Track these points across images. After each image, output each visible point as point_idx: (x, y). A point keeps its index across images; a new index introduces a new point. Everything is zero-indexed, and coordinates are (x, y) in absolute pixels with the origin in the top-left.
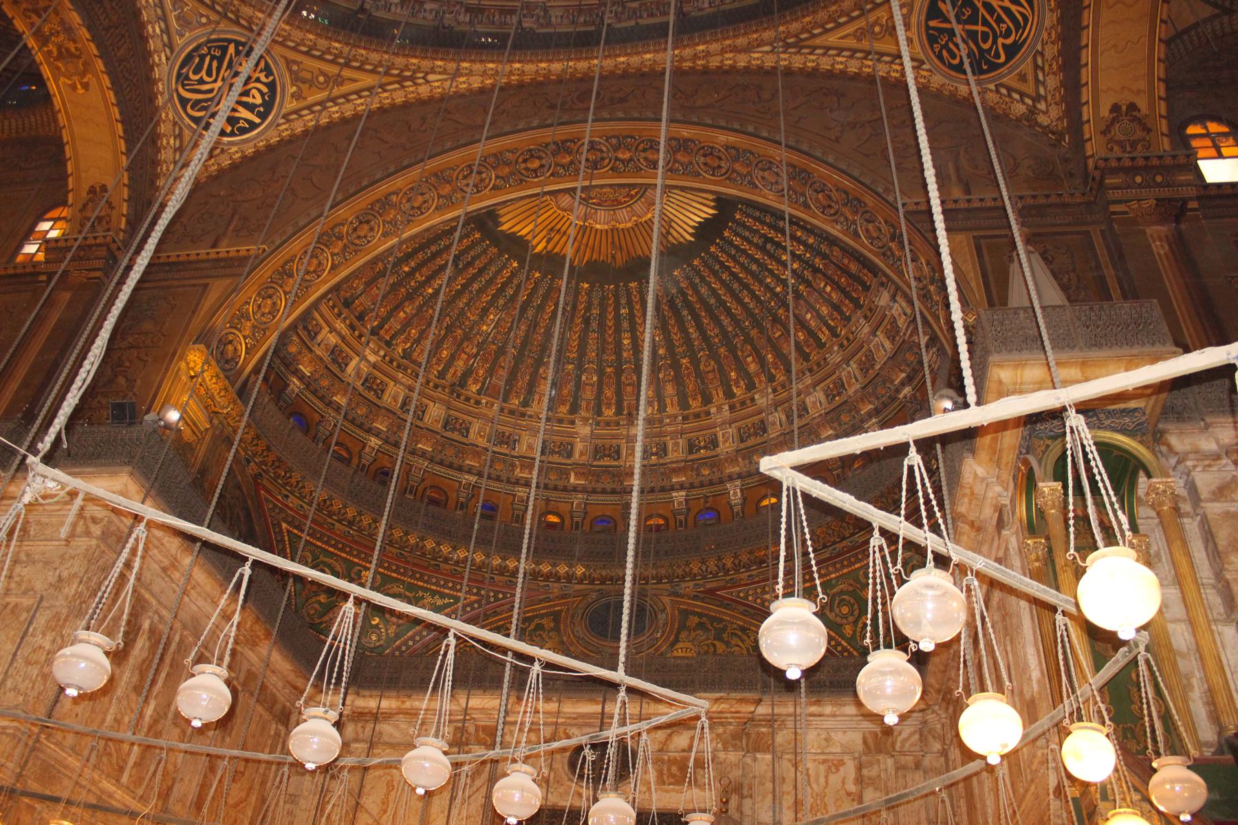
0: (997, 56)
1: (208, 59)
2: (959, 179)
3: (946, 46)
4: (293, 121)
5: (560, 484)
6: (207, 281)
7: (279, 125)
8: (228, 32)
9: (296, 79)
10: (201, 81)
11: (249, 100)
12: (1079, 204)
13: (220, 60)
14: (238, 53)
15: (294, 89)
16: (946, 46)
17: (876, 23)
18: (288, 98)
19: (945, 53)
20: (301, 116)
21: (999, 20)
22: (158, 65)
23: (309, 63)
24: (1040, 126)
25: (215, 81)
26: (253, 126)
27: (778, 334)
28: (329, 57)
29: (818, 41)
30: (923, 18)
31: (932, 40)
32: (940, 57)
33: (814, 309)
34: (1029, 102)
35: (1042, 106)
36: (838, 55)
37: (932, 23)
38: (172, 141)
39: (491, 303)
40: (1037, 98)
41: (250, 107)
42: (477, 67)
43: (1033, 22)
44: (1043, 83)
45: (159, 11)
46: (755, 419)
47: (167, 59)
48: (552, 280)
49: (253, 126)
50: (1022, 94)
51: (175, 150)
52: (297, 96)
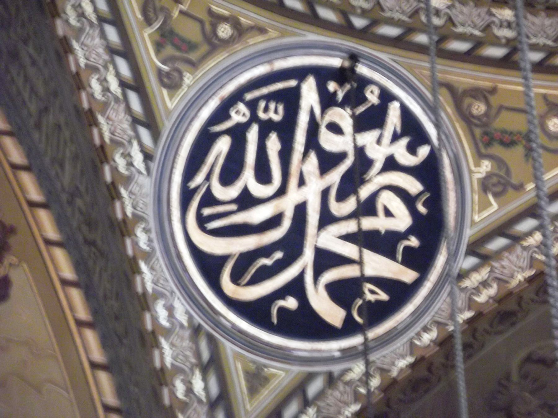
4: (498, 254)
7: (462, 275)
10: (246, 201)
13: (286, 130)
14: (327, 101)
15: (486, 166)
18: (473, 196)
20: (516, 239)
22: (128, 180)
23: (510, 84)
25: (282, 192)
26: (400, 293)
38: (198, 385)
45: (112, 33)
47: (148, 157)
49: (400, 293)
52: (497, 185)
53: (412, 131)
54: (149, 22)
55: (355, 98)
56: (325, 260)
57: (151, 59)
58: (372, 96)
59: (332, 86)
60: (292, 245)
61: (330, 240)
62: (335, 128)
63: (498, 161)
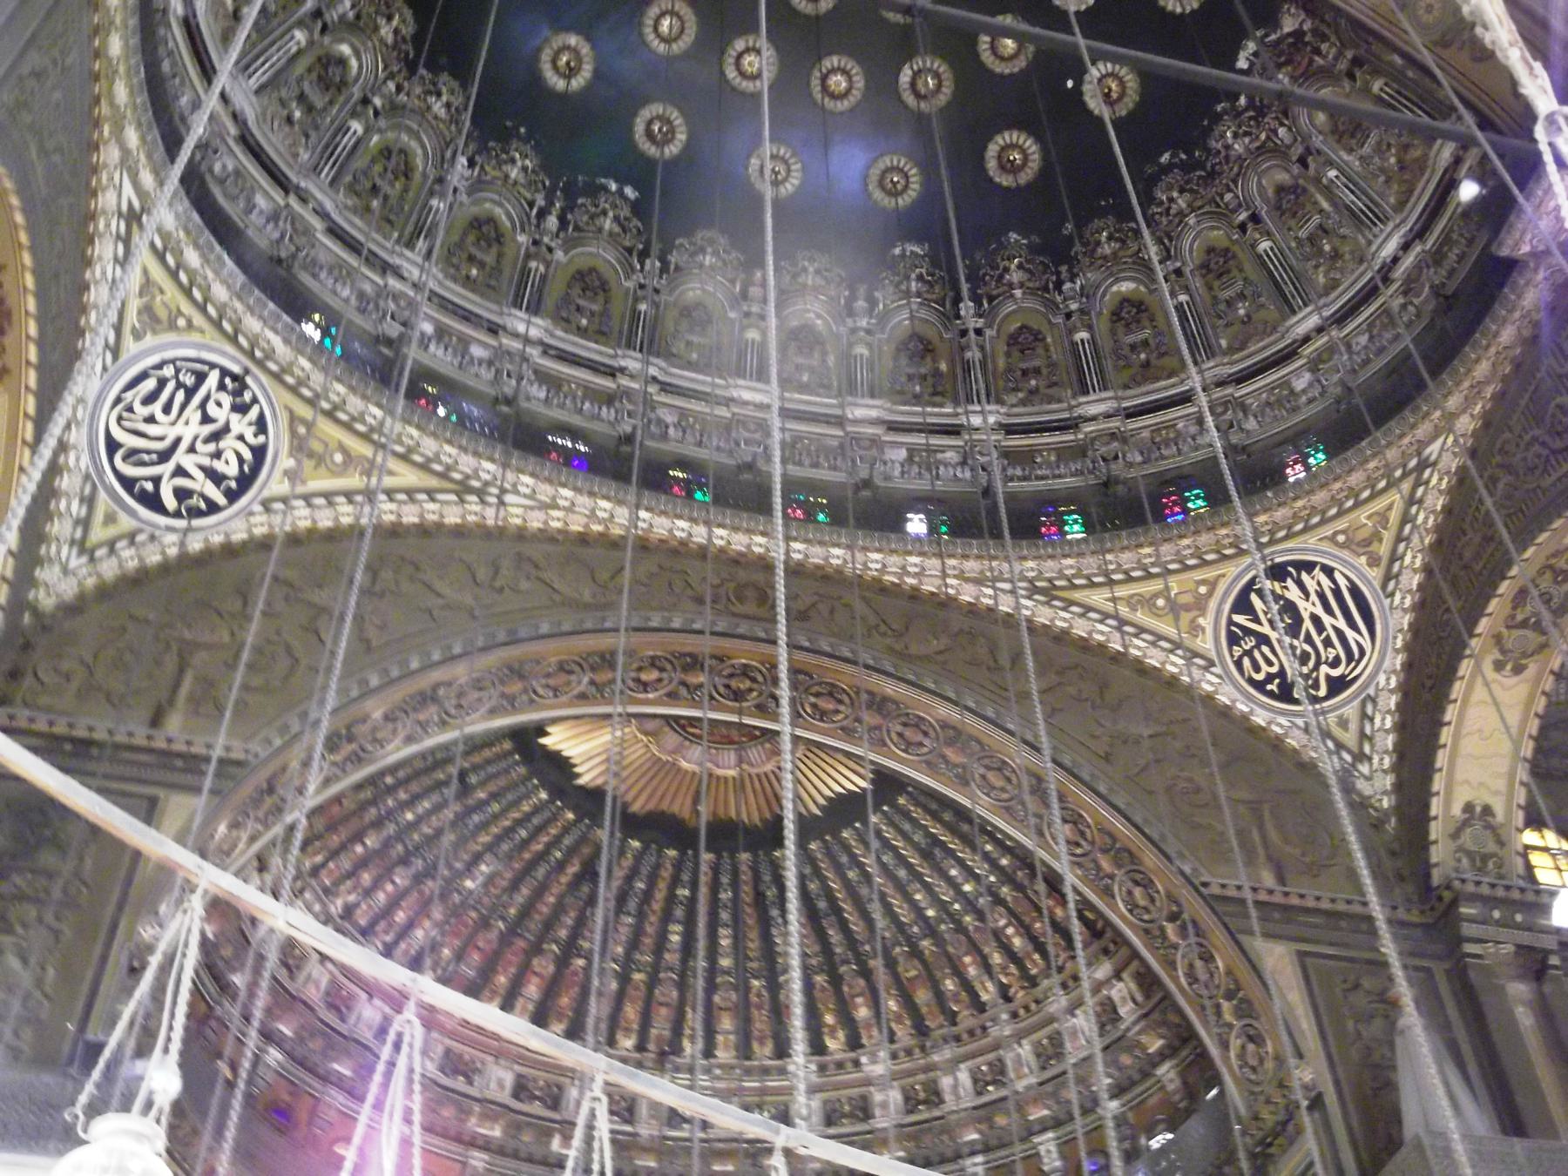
0: (1316, 686)
1: (171, 386)
2: (1270, 858)
5: (538, 1152)
6: (161, 793)
7: (251, 514)
8: (211, 349)
9: (299, 447)
11: (219, 466)
12: (1415, 925)
13: (190, 393)
14: (222, 387)
16: (1249, 653)
18: (277, 474)
19: (1246, 662)
21: (1328, 643)
24: (1359, 794)
26: (213, 508)
27: (913, 973)
28: (360, 428)
29: (1077, 595)
30: (1227, 607)
31: (1233, 640)
32: (1239, 664)
33: (979, 952)
34: (1348, 758)
35: (1364, 768)
36: (1101, 622)
37: (1239, 619)
39: (490, 848)
40: (1360, 757)
41: (216, 478)
42: (583, 501)
43: (1371, 658)
44: (1370, 739)
46: (855, 1092)
47: (105, 369)
48: (589, 827)
49: (213, 508)
50: (1340, 746)
51: (77, 522)
52: (292, 476)
53: (261, 425)
54: (141, 295)
55: (238, 393)
56: (180, 472)
57: (132, 317)
58: (247, 396)
59: (228, 381)
60: (164, 456)
61: (189, 462)
62: (219, 404)
63: (299, 462)
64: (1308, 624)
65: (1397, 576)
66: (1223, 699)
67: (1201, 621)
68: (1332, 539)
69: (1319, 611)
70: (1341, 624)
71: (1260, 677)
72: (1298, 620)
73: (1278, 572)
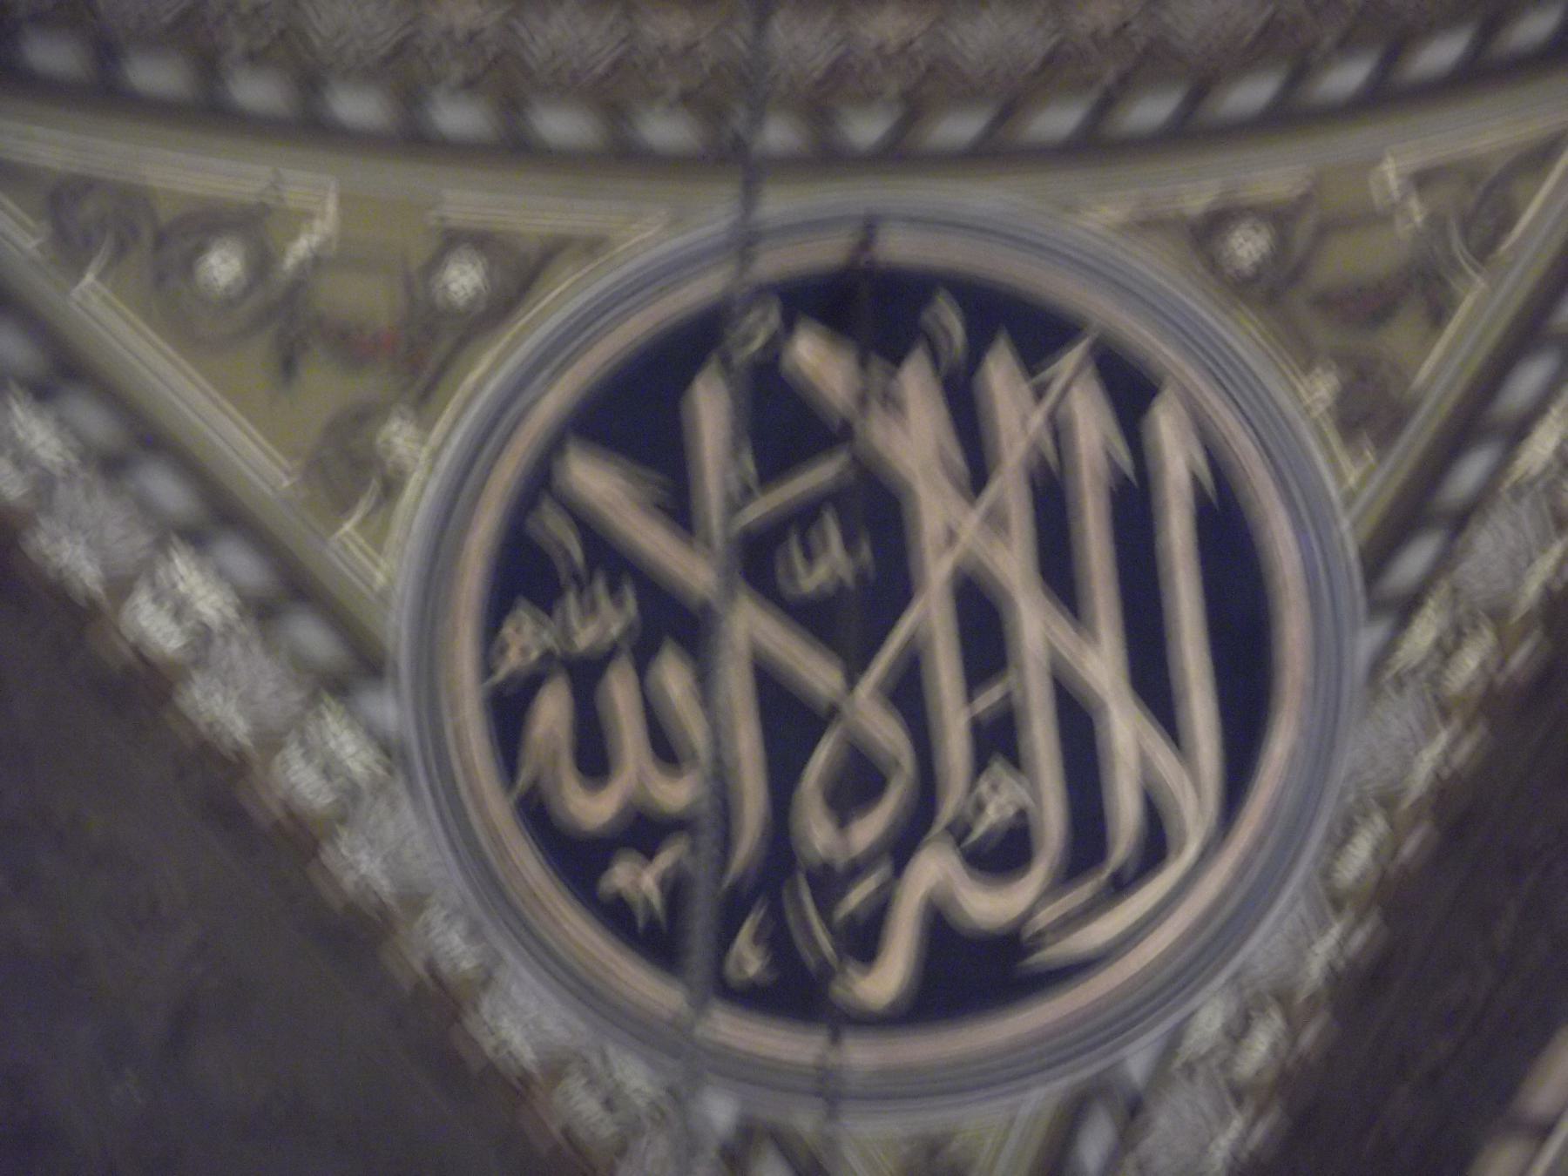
0: (864, 940)
3: (585, 675)
17: (251, 224)
19: (552, 712)
21: (998, 739)
30: (553, 402)
32: (509, 711)
37: (595, 480)
64: (931, 615)
65: (1461, 520)
66: (363, 863)
67: (399, 437)
68: (1207, 232)
69: (1013, 566)
70: (1103, 668)
71: (593, 809)
72: (891, 585)
73: (872, 306)
